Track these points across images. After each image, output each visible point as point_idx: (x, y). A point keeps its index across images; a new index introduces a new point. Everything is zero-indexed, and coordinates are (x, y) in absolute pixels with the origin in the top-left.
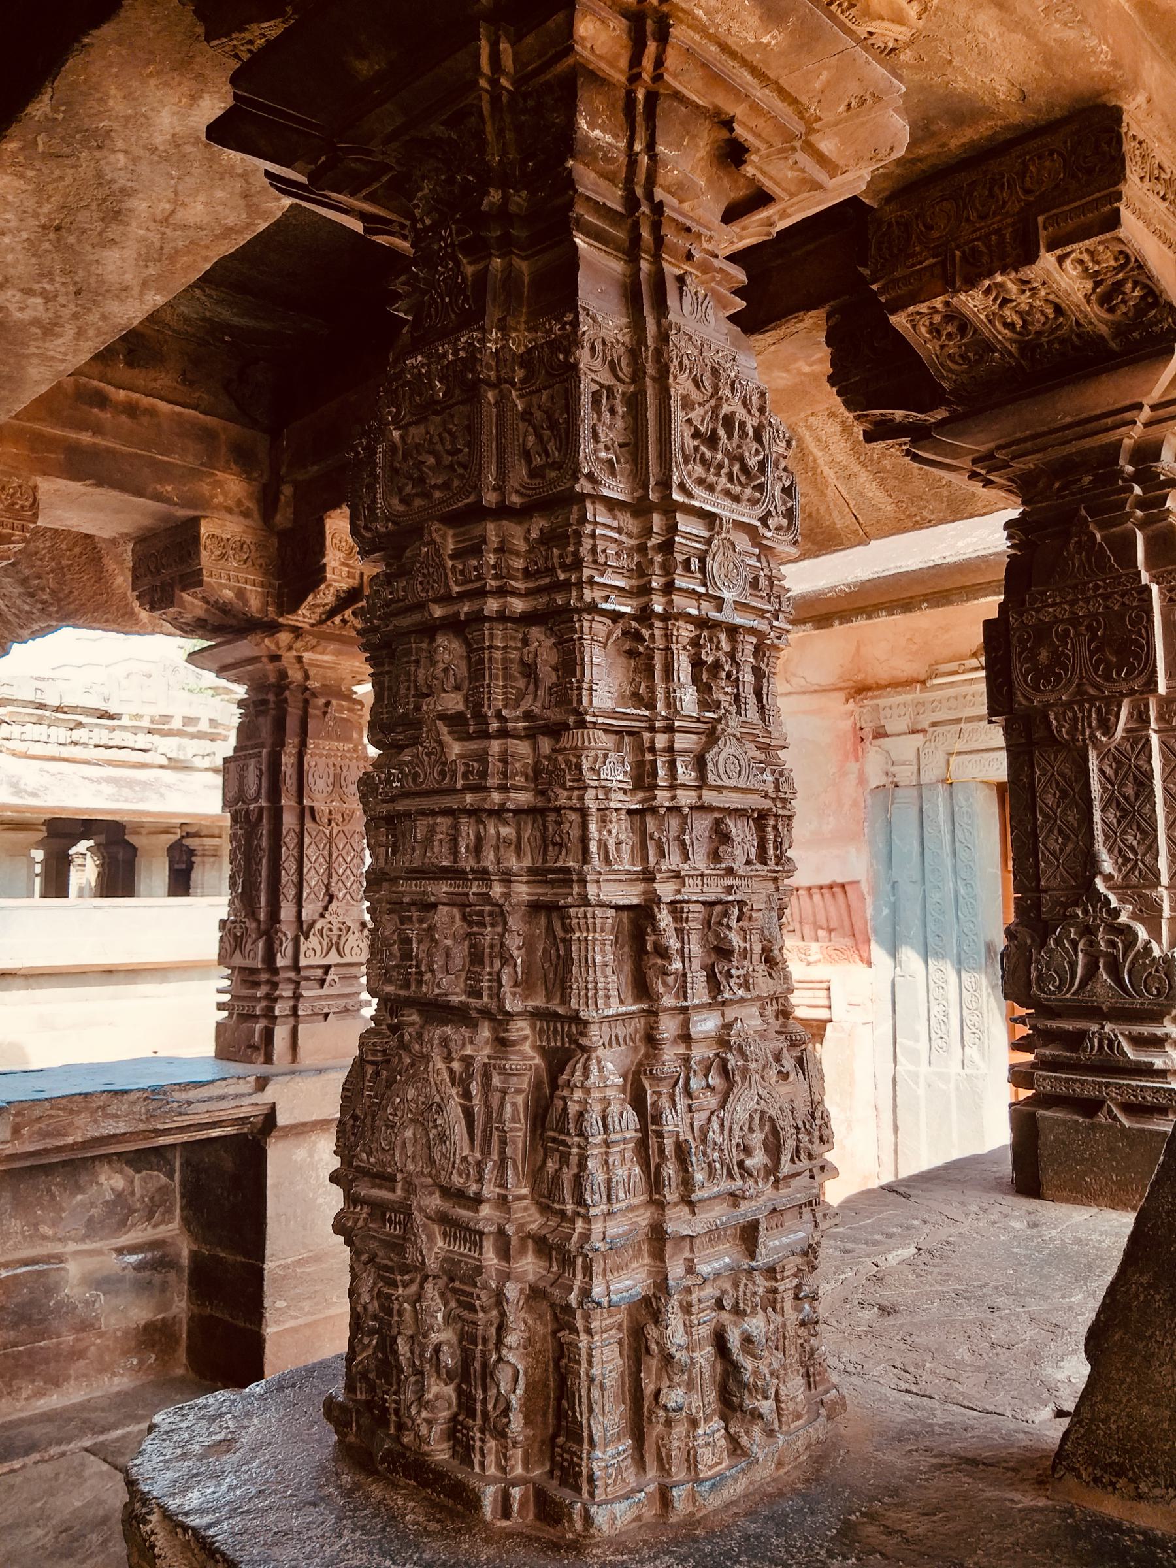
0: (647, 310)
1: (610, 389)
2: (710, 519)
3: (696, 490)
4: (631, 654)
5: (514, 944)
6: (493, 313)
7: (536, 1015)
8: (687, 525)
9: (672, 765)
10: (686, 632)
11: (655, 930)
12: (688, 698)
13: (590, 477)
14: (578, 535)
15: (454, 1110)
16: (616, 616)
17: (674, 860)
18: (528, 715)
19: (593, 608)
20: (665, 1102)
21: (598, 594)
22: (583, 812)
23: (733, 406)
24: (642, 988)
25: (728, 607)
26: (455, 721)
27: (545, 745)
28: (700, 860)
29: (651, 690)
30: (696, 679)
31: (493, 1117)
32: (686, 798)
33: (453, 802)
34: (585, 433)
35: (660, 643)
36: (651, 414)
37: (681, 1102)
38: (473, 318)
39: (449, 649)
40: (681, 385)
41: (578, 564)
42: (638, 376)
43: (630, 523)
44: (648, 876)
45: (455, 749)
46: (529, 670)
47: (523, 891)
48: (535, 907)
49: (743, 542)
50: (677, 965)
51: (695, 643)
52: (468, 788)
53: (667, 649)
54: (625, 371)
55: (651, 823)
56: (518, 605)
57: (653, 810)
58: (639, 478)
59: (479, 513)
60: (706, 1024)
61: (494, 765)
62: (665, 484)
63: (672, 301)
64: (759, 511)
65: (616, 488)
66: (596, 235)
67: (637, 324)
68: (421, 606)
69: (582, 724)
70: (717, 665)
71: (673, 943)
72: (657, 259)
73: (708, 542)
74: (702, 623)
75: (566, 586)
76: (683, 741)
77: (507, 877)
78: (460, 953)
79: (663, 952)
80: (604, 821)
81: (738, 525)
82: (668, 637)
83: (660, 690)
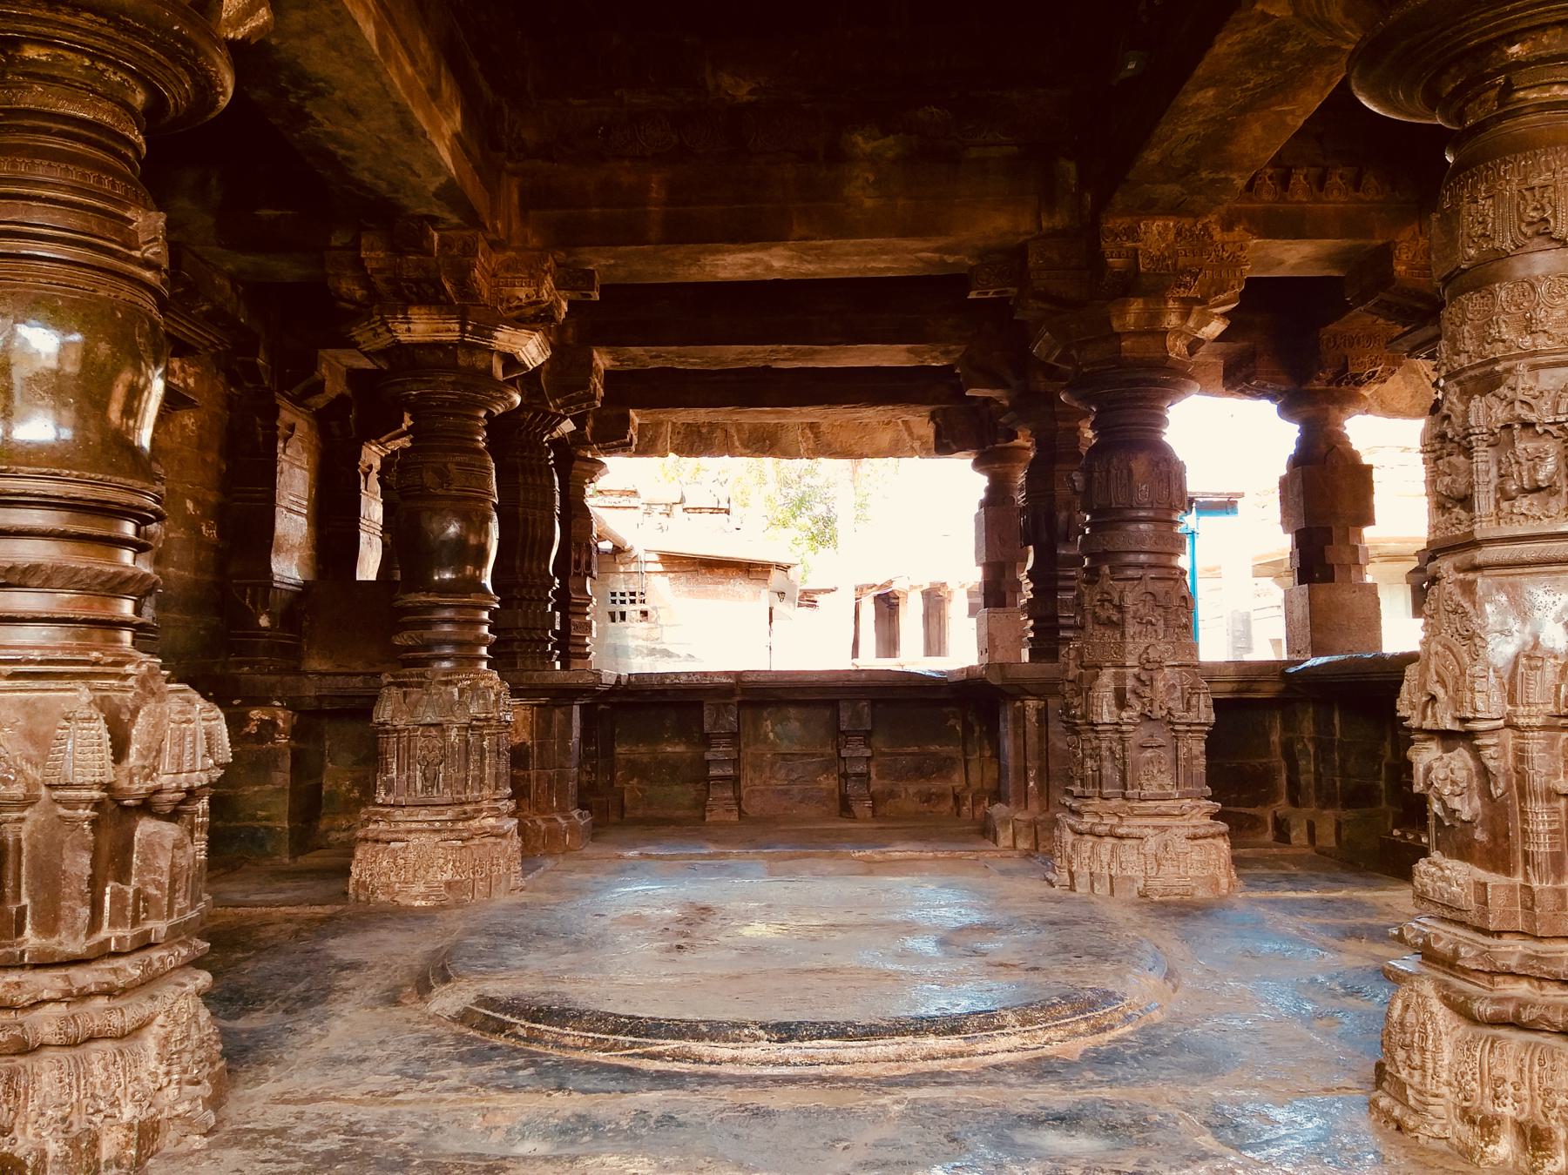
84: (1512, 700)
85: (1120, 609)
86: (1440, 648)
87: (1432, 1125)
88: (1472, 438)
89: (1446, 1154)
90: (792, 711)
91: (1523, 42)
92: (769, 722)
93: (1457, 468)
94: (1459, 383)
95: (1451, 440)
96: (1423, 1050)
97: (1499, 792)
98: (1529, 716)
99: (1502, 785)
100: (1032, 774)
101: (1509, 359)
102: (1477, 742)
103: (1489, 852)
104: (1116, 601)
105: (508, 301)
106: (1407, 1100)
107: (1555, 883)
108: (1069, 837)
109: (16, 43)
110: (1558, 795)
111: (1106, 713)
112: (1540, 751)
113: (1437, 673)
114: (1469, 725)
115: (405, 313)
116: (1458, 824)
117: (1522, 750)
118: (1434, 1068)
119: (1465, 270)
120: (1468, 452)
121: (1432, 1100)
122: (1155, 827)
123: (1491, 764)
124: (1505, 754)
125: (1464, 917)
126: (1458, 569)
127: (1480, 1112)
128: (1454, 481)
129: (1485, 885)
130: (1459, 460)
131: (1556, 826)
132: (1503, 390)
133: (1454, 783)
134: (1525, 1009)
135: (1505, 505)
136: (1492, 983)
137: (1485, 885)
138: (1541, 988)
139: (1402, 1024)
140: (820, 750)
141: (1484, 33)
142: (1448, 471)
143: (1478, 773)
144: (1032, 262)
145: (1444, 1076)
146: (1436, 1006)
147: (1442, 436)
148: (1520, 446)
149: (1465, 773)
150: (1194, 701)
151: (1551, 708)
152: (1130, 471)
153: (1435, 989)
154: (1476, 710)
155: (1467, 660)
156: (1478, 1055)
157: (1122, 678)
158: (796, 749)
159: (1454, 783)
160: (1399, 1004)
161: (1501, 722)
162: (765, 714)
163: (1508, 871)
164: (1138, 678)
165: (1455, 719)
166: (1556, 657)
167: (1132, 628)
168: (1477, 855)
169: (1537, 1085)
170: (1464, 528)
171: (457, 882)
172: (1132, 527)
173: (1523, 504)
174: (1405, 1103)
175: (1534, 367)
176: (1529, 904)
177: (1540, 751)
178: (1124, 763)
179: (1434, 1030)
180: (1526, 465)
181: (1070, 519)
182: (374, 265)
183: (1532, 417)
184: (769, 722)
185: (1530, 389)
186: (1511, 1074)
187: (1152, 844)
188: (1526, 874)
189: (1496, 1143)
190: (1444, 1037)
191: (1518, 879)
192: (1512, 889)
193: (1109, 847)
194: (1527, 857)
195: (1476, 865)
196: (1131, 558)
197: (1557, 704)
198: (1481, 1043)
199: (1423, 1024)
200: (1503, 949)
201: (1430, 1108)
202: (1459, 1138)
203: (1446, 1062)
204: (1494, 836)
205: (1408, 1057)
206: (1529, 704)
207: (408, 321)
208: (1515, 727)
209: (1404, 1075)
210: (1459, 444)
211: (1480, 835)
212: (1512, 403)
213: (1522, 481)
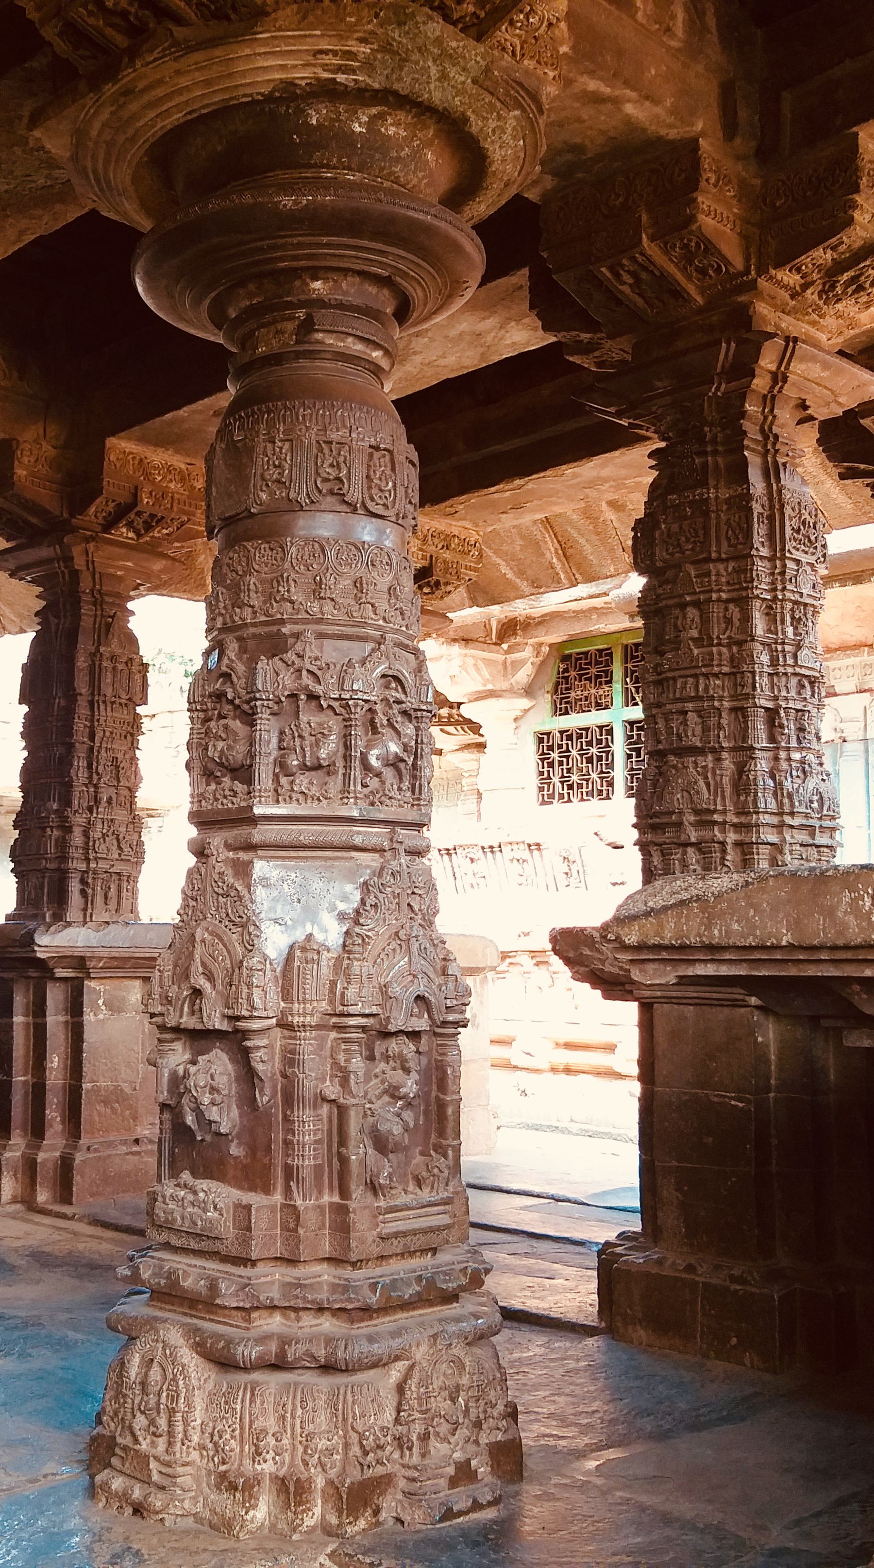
0: (773, 481)
1: (762, 514)
2: (798, 562)
3: (793, 551)
4: (767, 614)
5: (724, 722)
6: (712, 482)
7: (732, 749)
8: (790, 565)
9: (785, 656)
10: (789, 606)
11: (780, 718)
12: (790, 631)
13: (757, 549)
14: (752, 570)
15: (701, 783)
16: (764, 599)
17: (784, 693)
18: (729, 638)
19: (758, 597)
20: (783, 778)
21: (758, 592)
22: (753, 673)
23: (806, 516)
24: (772, 739)
25: (805, 595)
26: (698, 642)
27: (735, 649)
28: (793, 693)
29: (776, 628)
30: (792, 625)
31: (719, 785)
32: (790, 670)
33: (698, 671)
34: (755, 533)
35: (779, 610)
36: (777, 524)
37: (789, 779)
38: (704, 484)
39: (692, 613)
40: (788, 511)
41: (752, 580)
42: (772, 507)
43: (767, 564)
44: (776, 698)
45: (696, 652)
46: (729, 621)
47: (726, 704)
48: (733, 710)
49: (808, 569)
50: (786, 731)
51: (792, 610)
52: (704, 666)
53: (782, 613)
54: (767, 508)
55: (775, 679)
56: (724, 596)
57: (777, 674)
58: (773, 547)
59: (708, 560)
60: (796, 756)
61: (716, 656)
62: (783, 549)
63: (782, 475)
64: (815, 557)
65: (765, 552)
66: (753, 450)
67: (769, 486)
68: (681, 596)
69: (753, 640)
70: (800, 619)
71: (785, 723)
72: (774, 457)
73: (797, 571)
74: (796, 603)
75: (747, 588)
76: (788, 648)
77: (721, 698)
78: (698, 730)
79: (782, 726)
80: (761, 676)
81: (808, 563)
82: (782, 608)
83: (780, 628)
86: (206, 935)
87: (183, 1500)
88: (258, 703)
89: (197, 1534)
91: (326, 280)
93: (236, 734)
94: (240, 639)
95: (231, 702)
96: (172, 1412)
97: (266, 1099)
98: (305, 1014)
99: (268, 1091)
101: (295, 622)
102: (248, 1044)
103: (245, 1168)
106: (150, 1476)
107: (317, 1199)
110: (324, 1099)
112: (312, 1053)
113: (203, 964)
114: (241, 1024)
116: (208, 1138)
117: (293, 1052)
118: (185, 1432)
119: (253, 514)
120: (249, 718)
121: (180, 1470)
123: (260, 1067)
124: (273, 1058)
125: (218, 1246)
126: (229, 847)
127: (242, 1475)
128: (230, 748)
129: (248, 1208)
130: (236, 725)
131: (319, 1136)
133: (213, 1090)
134: (290, 1345)
135: (284, 780)
136: (249, 1320)
137: (248, 1208)
138: (298, 1320)
139: (144, 1384)
141: (295, 258)
142: (224, 736)
143: (237, 1079)
145: (196, 1438)
146: (188, 1357)
147: (219, 696)
148: (304, 718)
149: (225, 1078)
151: (324, 1006)
153: (183, 1336)
154: (253, 1008)
155: (240, 950)
156: (238, 1407)
159: (213, 1090)
160: (136, 1360)
161: (274, 1021)
163: (267, 1190)
165: (224, 1016)
166: (328, 950)
168: (231, 1173)
169: (298, 1430)
170: (240, 802)
173: (302, 781)
174: (147, 1481)
176: (292, 1225)
177: (312, 1053)
179: (186, 1386)
180: (309, 740)
185: (316, 659)
186: (271, 1423)
188: (288, 1191)
189: (254, 1507)
190: (196, 1392)
191: (278, 1198)
192: (273, 1209)
194: (290, 1173)
195: (230, 1184)
197: (331, 1002)
198: (241, 1393)
199: (174, 1379)
200: (263, 1279)
201: (179, 1480)
202: (213, 1511)
203: (199, 1422)
204: (253, 1149)
205: (152, 1422)
206: (305, 1001)
208: (289, 1027)
209: (144, 1446)
210: (239, 707)
211: (235, 1150)
212: (299, 671)
213: (305, 756)
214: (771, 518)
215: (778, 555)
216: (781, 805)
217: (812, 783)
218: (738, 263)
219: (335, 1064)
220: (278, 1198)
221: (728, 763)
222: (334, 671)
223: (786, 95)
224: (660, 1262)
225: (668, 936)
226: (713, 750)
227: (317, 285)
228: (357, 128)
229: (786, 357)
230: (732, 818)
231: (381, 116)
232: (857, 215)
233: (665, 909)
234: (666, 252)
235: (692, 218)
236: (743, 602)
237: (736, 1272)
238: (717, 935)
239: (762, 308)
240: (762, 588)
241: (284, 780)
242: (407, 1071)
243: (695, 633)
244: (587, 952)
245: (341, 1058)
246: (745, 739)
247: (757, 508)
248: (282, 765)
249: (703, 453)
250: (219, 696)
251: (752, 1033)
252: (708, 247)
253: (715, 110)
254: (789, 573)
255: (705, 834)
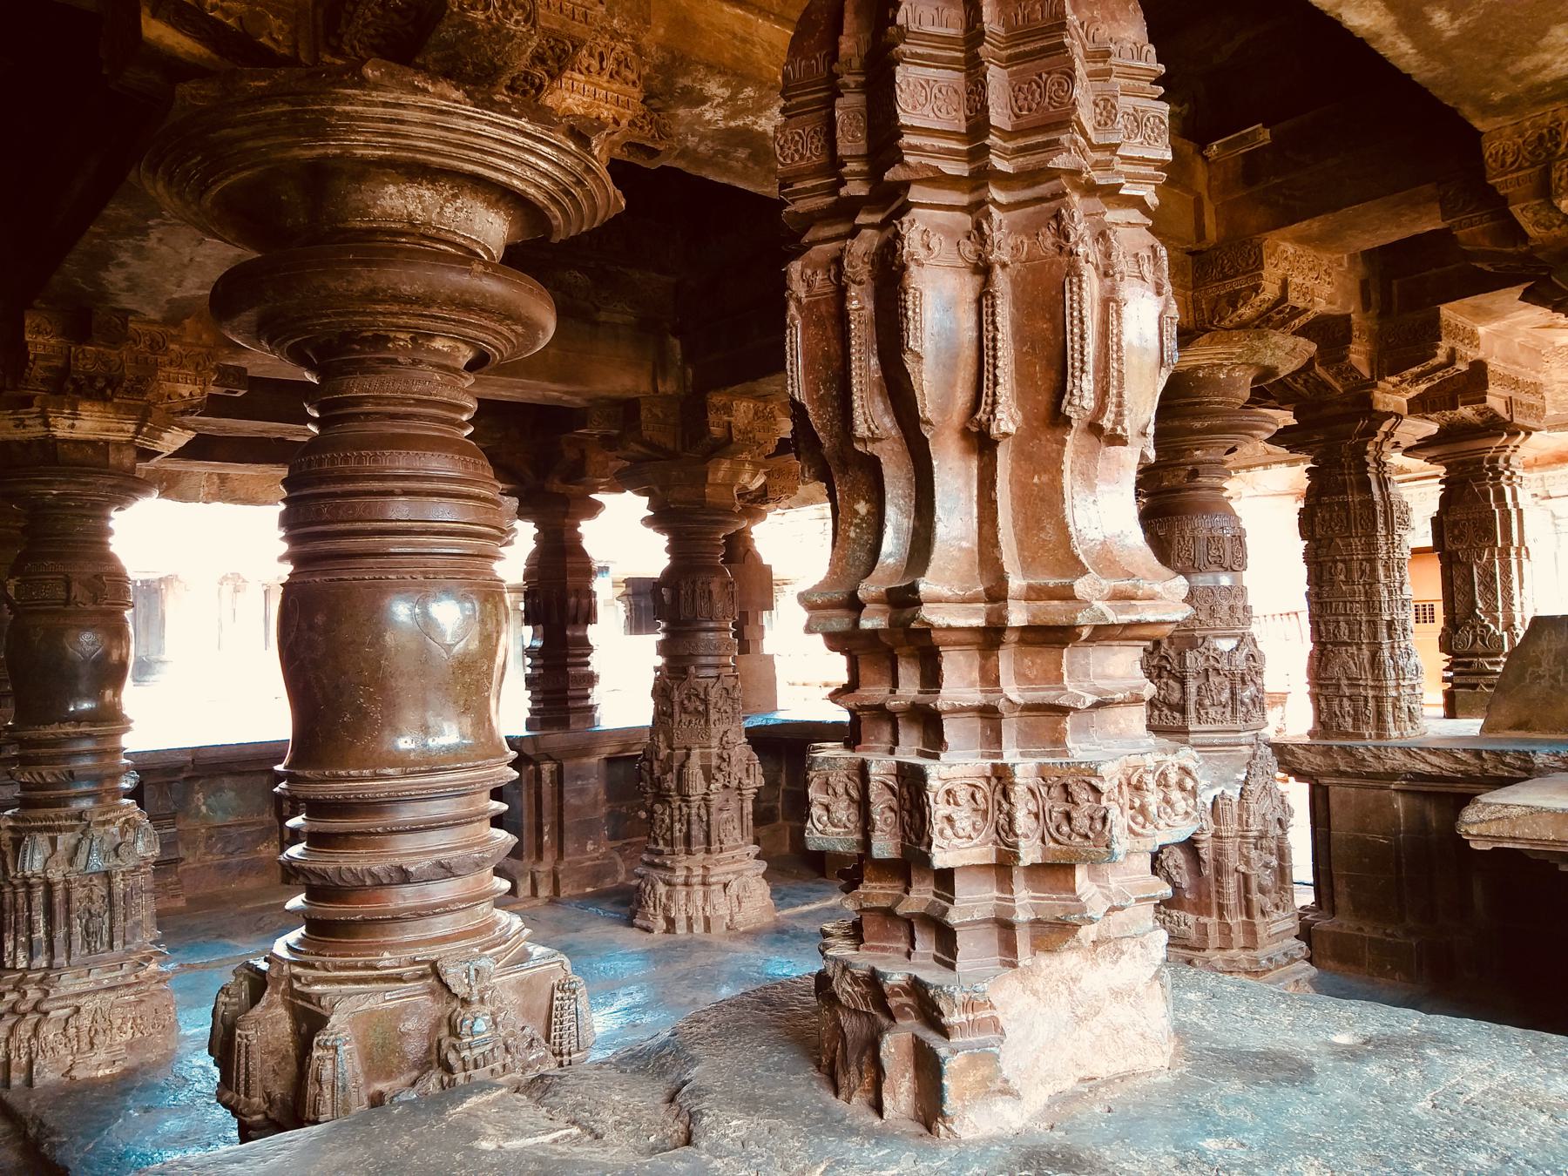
8: (1396, 537)
12: (1397, 574)
24: (1390, 637)
26: (1346, 583)
39: (1340, 565)
40: (1394, 508)
46: (1363, 572)
48: (1368, 621)
58: (1387, 529)
65: (1384, 533)
67: (1382, 493)
84: (1216, 822)
85: (705, 702)
90: (227, 781)
92: (200, 795)
100: (546, 829)
103: (1195, 904)
104: (702, 696)
105: (169, 397)
108: (662, 889)
109: (430, 337)
111: (697, 787)
115: (74, 408)
120: (1182, 682)
122: (734, 873)
125: (1186, 942)
132: (1202, 649)
133: (1177, 867)
140: (256, 818)
144: (644, 414)
150: (751, 771)
152: (710, 592)
157: (708, 756)
158: (231, 819)
159: (1177, 867)
162: (197, 787)
163: (1209, 915)
164: (721, 757)
167: (713, 716)
171: (139, 1040)
172: (703, 635)
175: (1216, 637)
178: (708, 824)
181: (578, 604)
182: (40, 350)
183: (1219, 666)
184: (200, 795)
187: (734, 889)
188: (1221, 916)
193: (701, 893)
196: (703, 660)
204: (1199, 895)
207: (75, 415)
208: (1221, 838)
214: (1385, 512)
215: (1390, 531)
216: (1397, 674)
217: (1412, 660)
218: (1367, 375)
219: (1242, 854)
220: (1215, 919)
221: (1366, 653)
222: (1225, 656)
223: (1395, 282)
224: (1341, 926)
225: (1493, 832)
226: (1357, 644)
227: (1198, 453)
228: (1222, 376)
229: (1395, 426)
230: (1370, 683)
231: (1233, 369)
232: (1439, 352)
233: (1490, 820)
234: (1327, 371)
235: (1346, 357)
236: (1372, 561)
237: (1388, 931)
238: (1517, 833)
239: (1377, 394)
240: (1382, 554)
241: (1202, 712)
242: (1272, 854)
243: (1342, 577)
244: (1289, 758)
245: (1245, 851)
246: (1375, 638)
247: (1378, 508)
248: (1200, 704)
249: (1344, 474)
250: (1161, 668)
251: (1391, 804)
252: (1353, 369)
253: (1358, 298)
254: (1397, 542)
255: (1355, 691)
